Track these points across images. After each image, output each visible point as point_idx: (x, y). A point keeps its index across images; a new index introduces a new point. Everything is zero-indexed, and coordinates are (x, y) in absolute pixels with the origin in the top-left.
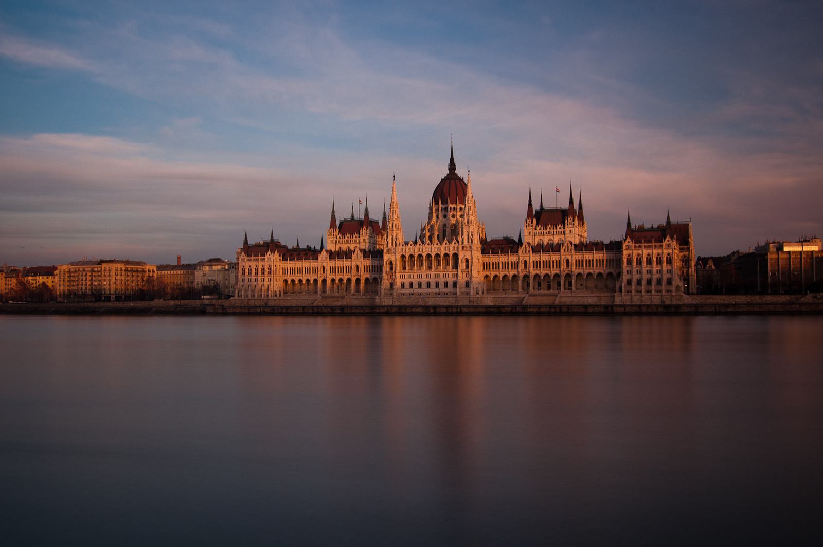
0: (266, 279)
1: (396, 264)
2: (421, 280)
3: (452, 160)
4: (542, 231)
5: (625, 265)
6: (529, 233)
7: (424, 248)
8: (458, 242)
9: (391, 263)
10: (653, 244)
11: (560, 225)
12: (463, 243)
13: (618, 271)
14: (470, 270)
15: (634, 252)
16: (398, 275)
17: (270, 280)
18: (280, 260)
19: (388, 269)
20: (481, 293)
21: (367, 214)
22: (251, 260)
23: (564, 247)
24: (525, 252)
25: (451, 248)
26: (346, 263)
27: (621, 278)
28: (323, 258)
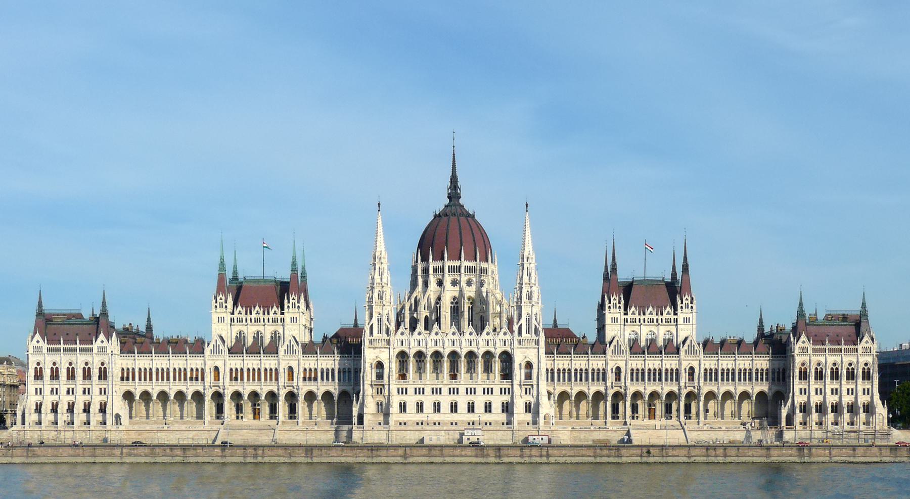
0: (95, 390)
1: (390, 368)
3: (454, 180)
4: (637, 317)
7: (463, 340)
8: (512, 332)
9: (380, 365)
10: (843, 347)
11: (668, 309)
13: (775, 389)
14: (535, 383)
17: (103, 392)
19: (374, 378)
21: (294, 271)
23: (686, 347)
24: (618, 351)
25: (498, 342)
27: (790, 400)
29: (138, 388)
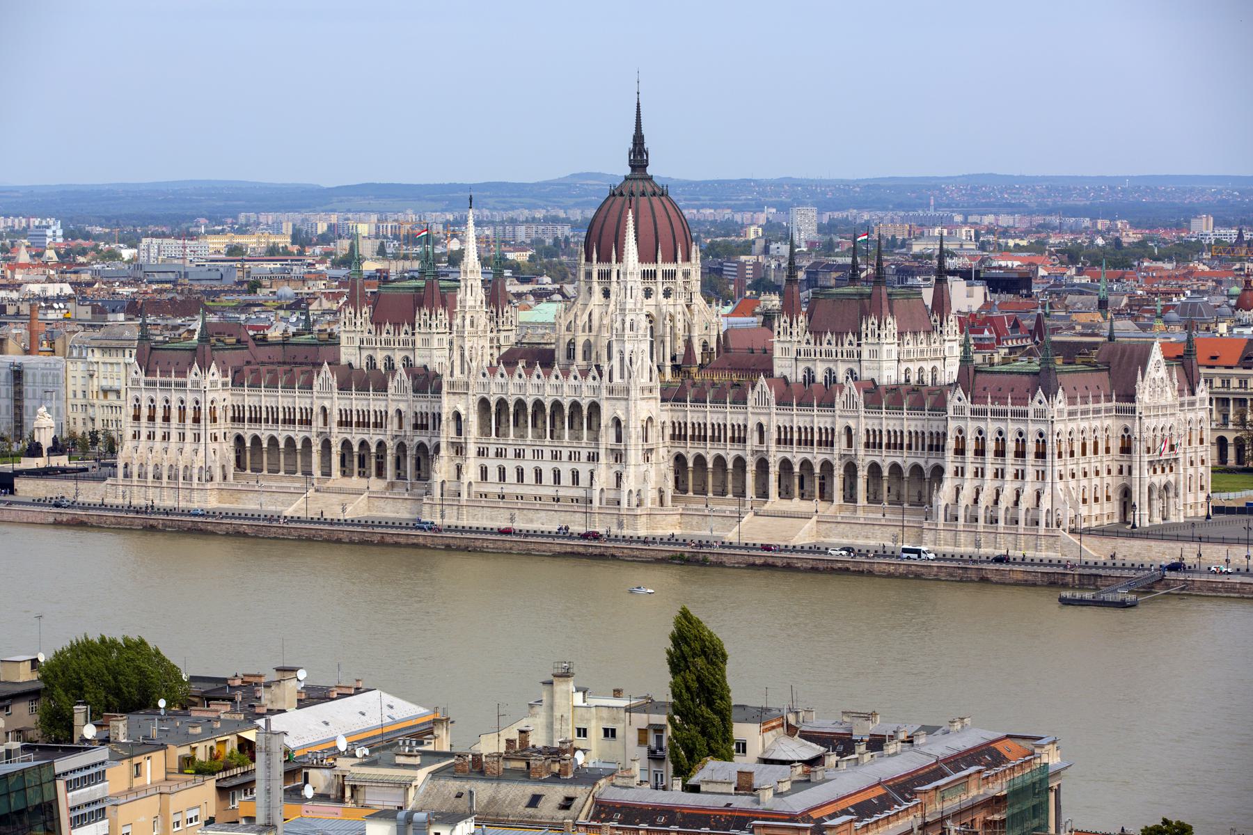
2: (523, 464)
3: (638, 139)
5: (950, 454)
6: (785, 351)
8: (601, 376)
9: (457, 416)
10: (1010, 407)
12: (611, 380)
15: (970, 423)
16: (472, 450)
17: (197, 438)
18: (224, 384)
19: (453, 433)
20: (648, 503)
22: (154, 384)
26: (370, 403)
28: (326, 386)
29: (248, 432)
